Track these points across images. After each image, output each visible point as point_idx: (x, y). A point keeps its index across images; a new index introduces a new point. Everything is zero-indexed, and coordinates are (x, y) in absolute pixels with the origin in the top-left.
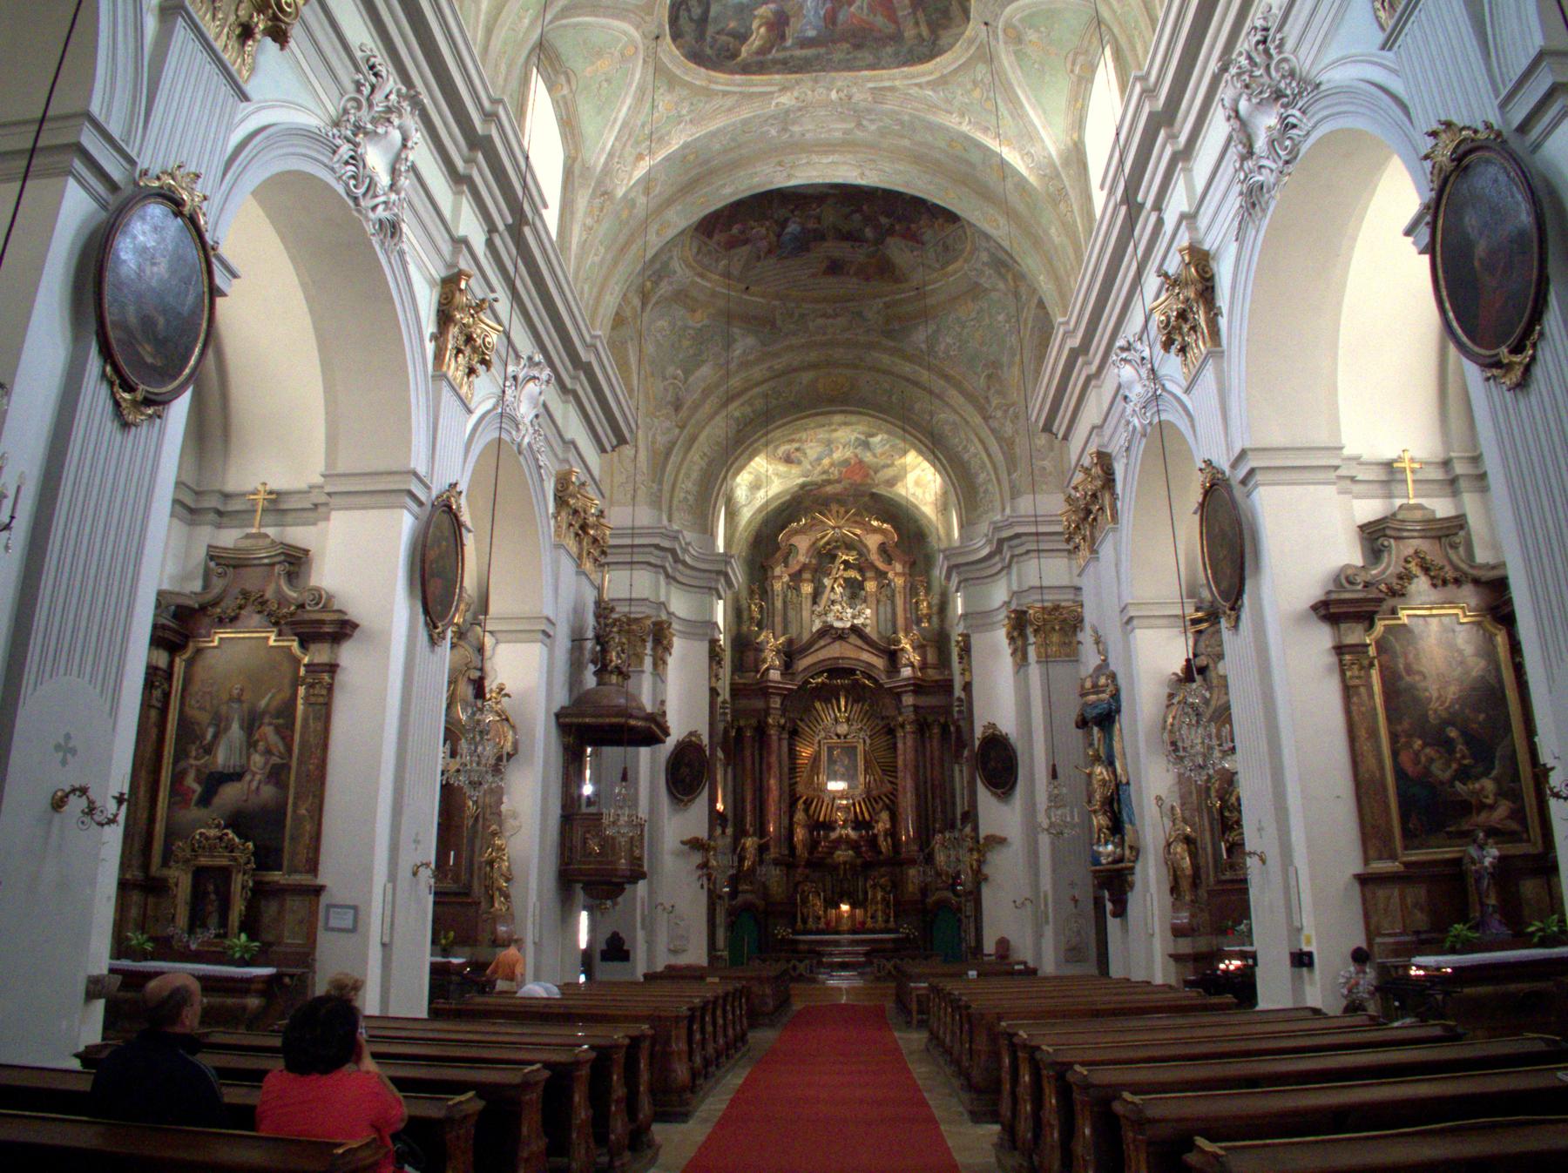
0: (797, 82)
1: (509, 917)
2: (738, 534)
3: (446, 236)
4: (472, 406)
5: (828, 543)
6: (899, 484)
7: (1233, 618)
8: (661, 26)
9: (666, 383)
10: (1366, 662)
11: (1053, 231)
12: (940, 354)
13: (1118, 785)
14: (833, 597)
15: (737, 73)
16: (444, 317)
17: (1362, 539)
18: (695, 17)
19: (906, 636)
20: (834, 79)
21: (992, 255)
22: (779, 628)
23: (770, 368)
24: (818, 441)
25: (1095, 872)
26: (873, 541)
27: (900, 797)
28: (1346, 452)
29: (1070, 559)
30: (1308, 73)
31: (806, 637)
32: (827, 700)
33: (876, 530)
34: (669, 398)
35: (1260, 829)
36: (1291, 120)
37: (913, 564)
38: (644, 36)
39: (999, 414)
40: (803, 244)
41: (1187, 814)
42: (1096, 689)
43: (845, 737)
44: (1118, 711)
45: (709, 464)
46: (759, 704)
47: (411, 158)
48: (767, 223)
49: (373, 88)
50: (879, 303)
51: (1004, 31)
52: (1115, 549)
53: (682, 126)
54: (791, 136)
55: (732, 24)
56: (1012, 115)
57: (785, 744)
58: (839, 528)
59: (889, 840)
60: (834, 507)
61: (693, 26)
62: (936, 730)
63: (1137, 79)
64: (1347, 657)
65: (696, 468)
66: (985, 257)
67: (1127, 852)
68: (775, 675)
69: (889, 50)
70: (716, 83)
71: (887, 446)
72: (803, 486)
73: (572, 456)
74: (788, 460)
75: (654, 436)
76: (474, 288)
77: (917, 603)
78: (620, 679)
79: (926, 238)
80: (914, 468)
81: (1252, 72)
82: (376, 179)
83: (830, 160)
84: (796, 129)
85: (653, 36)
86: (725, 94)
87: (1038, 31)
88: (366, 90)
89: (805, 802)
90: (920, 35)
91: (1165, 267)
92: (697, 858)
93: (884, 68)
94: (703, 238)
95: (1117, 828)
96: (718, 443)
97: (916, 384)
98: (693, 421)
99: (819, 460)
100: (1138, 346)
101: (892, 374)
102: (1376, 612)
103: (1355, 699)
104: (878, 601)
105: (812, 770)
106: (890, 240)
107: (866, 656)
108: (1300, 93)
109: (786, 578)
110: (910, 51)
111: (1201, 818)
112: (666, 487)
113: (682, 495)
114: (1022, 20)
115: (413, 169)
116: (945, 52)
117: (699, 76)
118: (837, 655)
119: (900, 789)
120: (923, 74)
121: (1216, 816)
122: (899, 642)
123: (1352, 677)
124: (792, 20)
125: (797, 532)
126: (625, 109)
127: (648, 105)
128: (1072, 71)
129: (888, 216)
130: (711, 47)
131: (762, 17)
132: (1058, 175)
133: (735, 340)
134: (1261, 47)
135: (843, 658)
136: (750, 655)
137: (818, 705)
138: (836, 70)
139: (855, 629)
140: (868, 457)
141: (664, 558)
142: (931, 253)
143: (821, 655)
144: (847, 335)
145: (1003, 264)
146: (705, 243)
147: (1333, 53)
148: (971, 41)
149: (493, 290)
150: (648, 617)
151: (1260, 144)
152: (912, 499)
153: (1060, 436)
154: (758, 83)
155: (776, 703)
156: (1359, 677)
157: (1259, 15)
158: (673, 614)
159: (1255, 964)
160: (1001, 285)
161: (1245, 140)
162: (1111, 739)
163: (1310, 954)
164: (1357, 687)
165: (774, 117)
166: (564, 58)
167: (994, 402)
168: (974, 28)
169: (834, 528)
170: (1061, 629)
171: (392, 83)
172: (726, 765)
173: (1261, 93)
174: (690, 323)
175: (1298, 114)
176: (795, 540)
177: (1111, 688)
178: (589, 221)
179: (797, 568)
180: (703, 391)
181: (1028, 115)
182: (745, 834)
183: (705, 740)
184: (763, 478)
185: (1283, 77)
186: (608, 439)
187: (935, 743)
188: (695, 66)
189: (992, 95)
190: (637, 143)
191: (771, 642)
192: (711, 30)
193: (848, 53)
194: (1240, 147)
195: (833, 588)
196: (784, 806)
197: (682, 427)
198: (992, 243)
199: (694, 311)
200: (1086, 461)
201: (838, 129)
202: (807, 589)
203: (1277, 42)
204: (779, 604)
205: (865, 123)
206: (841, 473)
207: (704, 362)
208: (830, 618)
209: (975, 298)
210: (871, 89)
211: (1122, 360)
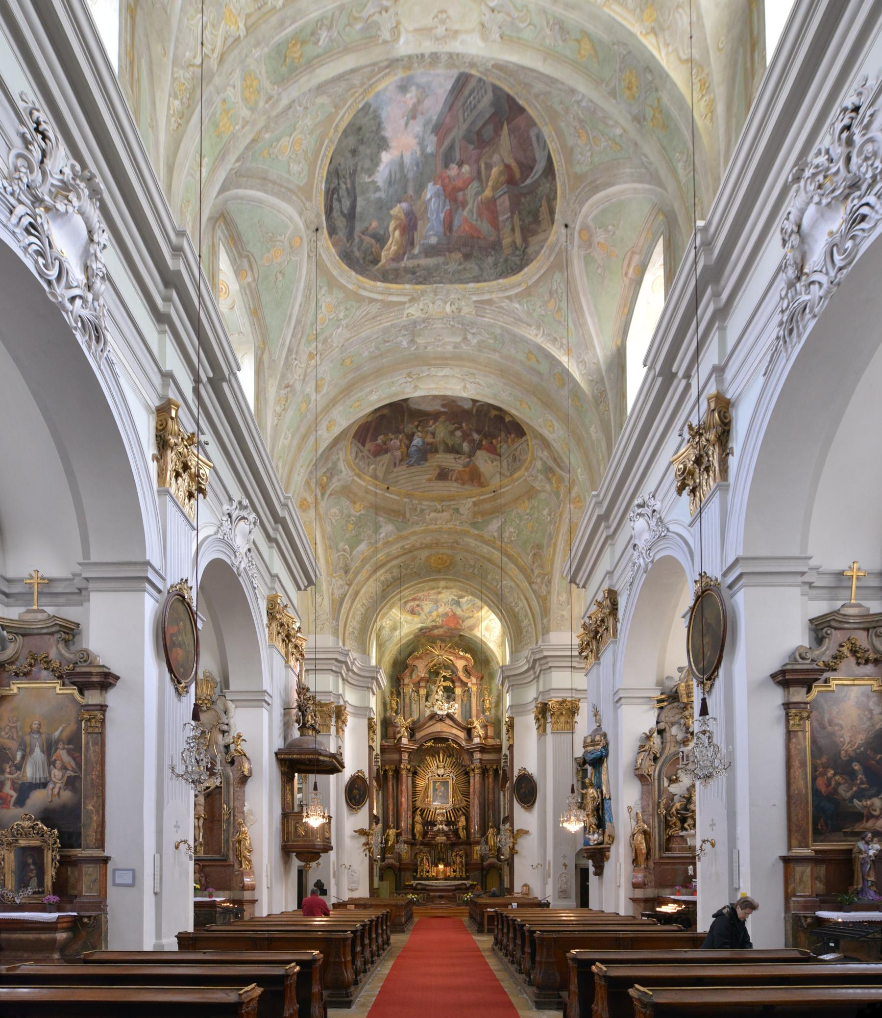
11: (592, 429)
20: (448, 293)
22: (407, 715)
24: (431, 600)
34: (341, 565)
38: (307, 227)
45: (366, 611)
50: (469, 502)
54: (417, 348)
55: (374, 224)
56: (575, 325)
61: (344, 219)
65: (358, 613)
66: (539, 465)
69: (490, 260)
70: (364, 289)
71: (470, 605)
74: (412, 612)
79: (503, 451)
84: (421, 341)
85: (314, 228)
86: (372, 300)
93: (485, 281)
94: (360, 445)
95: (601, 824)
98: (356, 581)
99: (430, 612)
106: (479, 453)
112: (341, 624)
117: (349, 278)
121: (663, 819)
124: (420, 223)
126: (297, 307)
129: (479, 432)
130: (359, 250)
131: (397, 218)
132: (602, 379)
140: (459, 612)
142: (505, 463)
146: (361, 451)
160: (548, 487)
165: (405, 327)
166: (244, 239)
167: (536, 572)
168: (557, 233)
174: (353, 512)
181: (586, 322)
188: (347, 268)
191: (402, 722)
192: (358, 227)
193: (460, 264)
197: (350, 585)
205: (469, 336)
206: (443, 621)
209: (530, 498)
210: (475, 302)
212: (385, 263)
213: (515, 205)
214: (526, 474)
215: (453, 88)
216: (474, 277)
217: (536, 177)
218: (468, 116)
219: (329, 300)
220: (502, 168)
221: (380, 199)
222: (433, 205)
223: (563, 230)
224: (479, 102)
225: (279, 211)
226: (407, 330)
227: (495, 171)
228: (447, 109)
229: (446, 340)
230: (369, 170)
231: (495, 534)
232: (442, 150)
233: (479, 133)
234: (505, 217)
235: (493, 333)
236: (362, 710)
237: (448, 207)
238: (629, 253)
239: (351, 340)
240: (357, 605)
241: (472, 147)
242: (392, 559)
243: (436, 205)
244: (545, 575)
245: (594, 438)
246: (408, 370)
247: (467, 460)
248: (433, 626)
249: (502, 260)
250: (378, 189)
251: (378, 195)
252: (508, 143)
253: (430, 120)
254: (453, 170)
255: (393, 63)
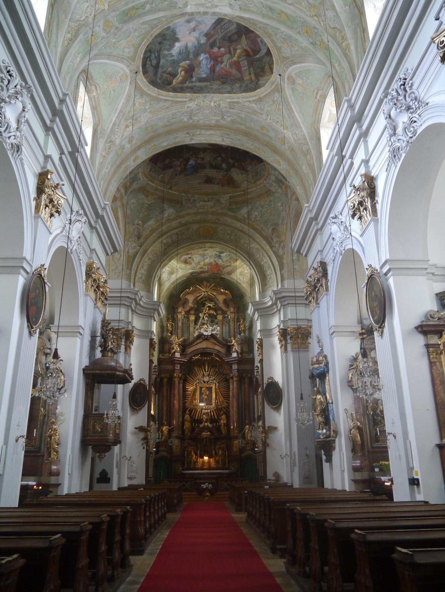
0: (197, 97)
1: (57, 462)
2: (162, 294)
3: (42, 154)
4: (52, 231)
5: (202, 298)
6: (233, 274)
7: (380, 331)
8: (138, 67)
9: (134, 227)
10: (439, 352)
11: (304, 167)
12: (253, 219)
13: (328, 404)
14: (203, 322)
15: (171, 92)
16: (40, 190)
17: (437, 299)
18: (153, 64)
19: (234, 339)
21: (276, 178)
22: (180, 335)
23: (180, 222)
25: (318, 442)
26: (221, 298)
27: (231, 409)
28: (430, 262)
29: (305, 307)
30: (423, 98)
31: (191, 339)
32: (200, 367)
33: (222, 293)
35: (393, 423)
36: (414, 119)
37: (238, 308)
38: (131, 71)
39: (277, 245)
40: (197, 168)
41: (358, 417)
42: (318, 362)
43: (207, 382)
44: (328, 372)
45: (152, 262)
46: (170, 367)
47: (26, 116)
48: (181, 160)
49: (9, 81)
50: (228, 196)
51: (288, 79)
52: (327, 303)
53: (146, 114)
54: (193, 121)
55: (170, 69)
57: (181, 385)
58: (207, 292)
59: (226, 428)
60: (205, 283)
61: (152, 68)
62: (246, 380)
63: (346, 100)
64: (431, 349)
65: (146, 264)
66: (273, 178)
67: (332, 433)
68: (178, 355)
69: (237, 85)
70: (162, 95)
71: (228, 258)
72: (192, 273)
73: (94, 256)
74: (186, 262)
75: (128, 249)
76: (53, 178)
77: (239, 325)
78: (112, 354)
80: (239, 267)
81: (398, 98)
82: (10, 124)
83: (209, 133)
84: (195, 118)
85: (135, 72)
86: (166, 100)
87: (302, 79)
88: (6, 82)
89: (189, 411)
90: (251, 79)
91: (354, 183)
92: (142, 435)
93: (235, 93)
96: (156, 254)
97: (242, 231)
98: (145, 244)
99: (199, 263)
100: (340, 217)
101: (231, 226)
102: (443, 331)
103: (434, 367)
104: (223, 324)
105: (193, 396)
106: (233, 170)
107: (217, 348)
108: (419, 107)
109: (183, 313)
110: (246, 86)
111: (364, 419)
113: (140, 276)
114: (295, 74)
115: (27, 122)
116: (262, 87)
117: (154, 91)
118: (205, 347)
119: (231, 405)
120: (251, 97)
122: (232, 342)
123: (433, 358)
124: (196, 69)
125: (188, 293)
127: (131, 103)
128: (316, 98)
131: (182, 67)
133: (165, 210)
134: (402, 87)
135: (207, 348)
136: (167, 347)
137: (196, 368)
138: (214, 93)
139: (212, 335)
140: (220, 262)
141: (131, 303)
142: (250, 176)
143: (198, 347)
144: (213, 210)
145: (281, 181)
147: (434, 90)
148: (273, 83)
149: (62, 181)
150: (123, 328)
151: (400, 130)
152: (238, 280)
153: (304, 255)
154: (180, 97)
155: (178, 367)
156: (436, 358)
157: (402, 72)
158: (134, 327)
159: (392, 483)
160: (280, 190)
161: (393, 128)
162: (324, 384)
163: (418, 480)
164: (435, 362)
165: (186, 112)
166: (94, 78)
167: (275, 240)
168: (275, 77)
169: (205, 292)
170: (301, 337)
171: (17, 80)
172: (155, 395)
173: (401, 107)
174: (146, 201)
175: (417, 116)
176: (188, 297)
177: (325, 361)
178: (104, 154)
179: (188, 309)
180: (150, 231)
182: (163, 425)
183: (147, 382)
184: (175, 270)
185: (412, 100)
186: (110, 250)
187: (246, 385)
189: (281, 107)
190: (126, 120)
191: (176, 340)
192: (160, 71)
193: (220, 86)
194: (390, 131)
195: (203, 318)
196: (181, 413)
197: (141, 246)
198: (277, 172)
199: (147, 196)
200: (315, 265)
201: (213, 120)
202: (192, 318)
203: (410, 85)
204: (180, 324)
205: (225, 117)
206: (208, 268)
207: (151, 218)
208: (202, 331)
211: (333, 222)
212: (175, 85)
213: (251, 64)
214: (265, 182)
215: (215, 22)
216: (228, 92)
217: (262, 55)
218: (223, 31)
219: (140, 101)
220: (243, 50)
221: (174, 60)
222: (204, 62)
223: (279, 77)
224: (229, 27)
225: (116, 67)
226: (187, 113)
227: (238, 51)
228: (212, 28)
229: (211, 118)
230: (168, 49)
231: (246, 216)
232: (209, 43)
233: (230, 38)
234: (245, 68)
235: (239, 116)
236: (147, 333)
237: (212, 63)
238: (316, 90)
239: (152, 118)
240: (146, 259)
241: (226, 42)
242: (172, 230)
243: (206, 62)
244: (281, 242)
245: (305, 172)
246: (187, 131)
247: (225, 173)
248: (201, 272)
249: (244, 85)
250: (173, 56)
251: (172, 58)
252: (246, 42)
253: (203, 32)
254: (215, 50)
255: (183, 15)
